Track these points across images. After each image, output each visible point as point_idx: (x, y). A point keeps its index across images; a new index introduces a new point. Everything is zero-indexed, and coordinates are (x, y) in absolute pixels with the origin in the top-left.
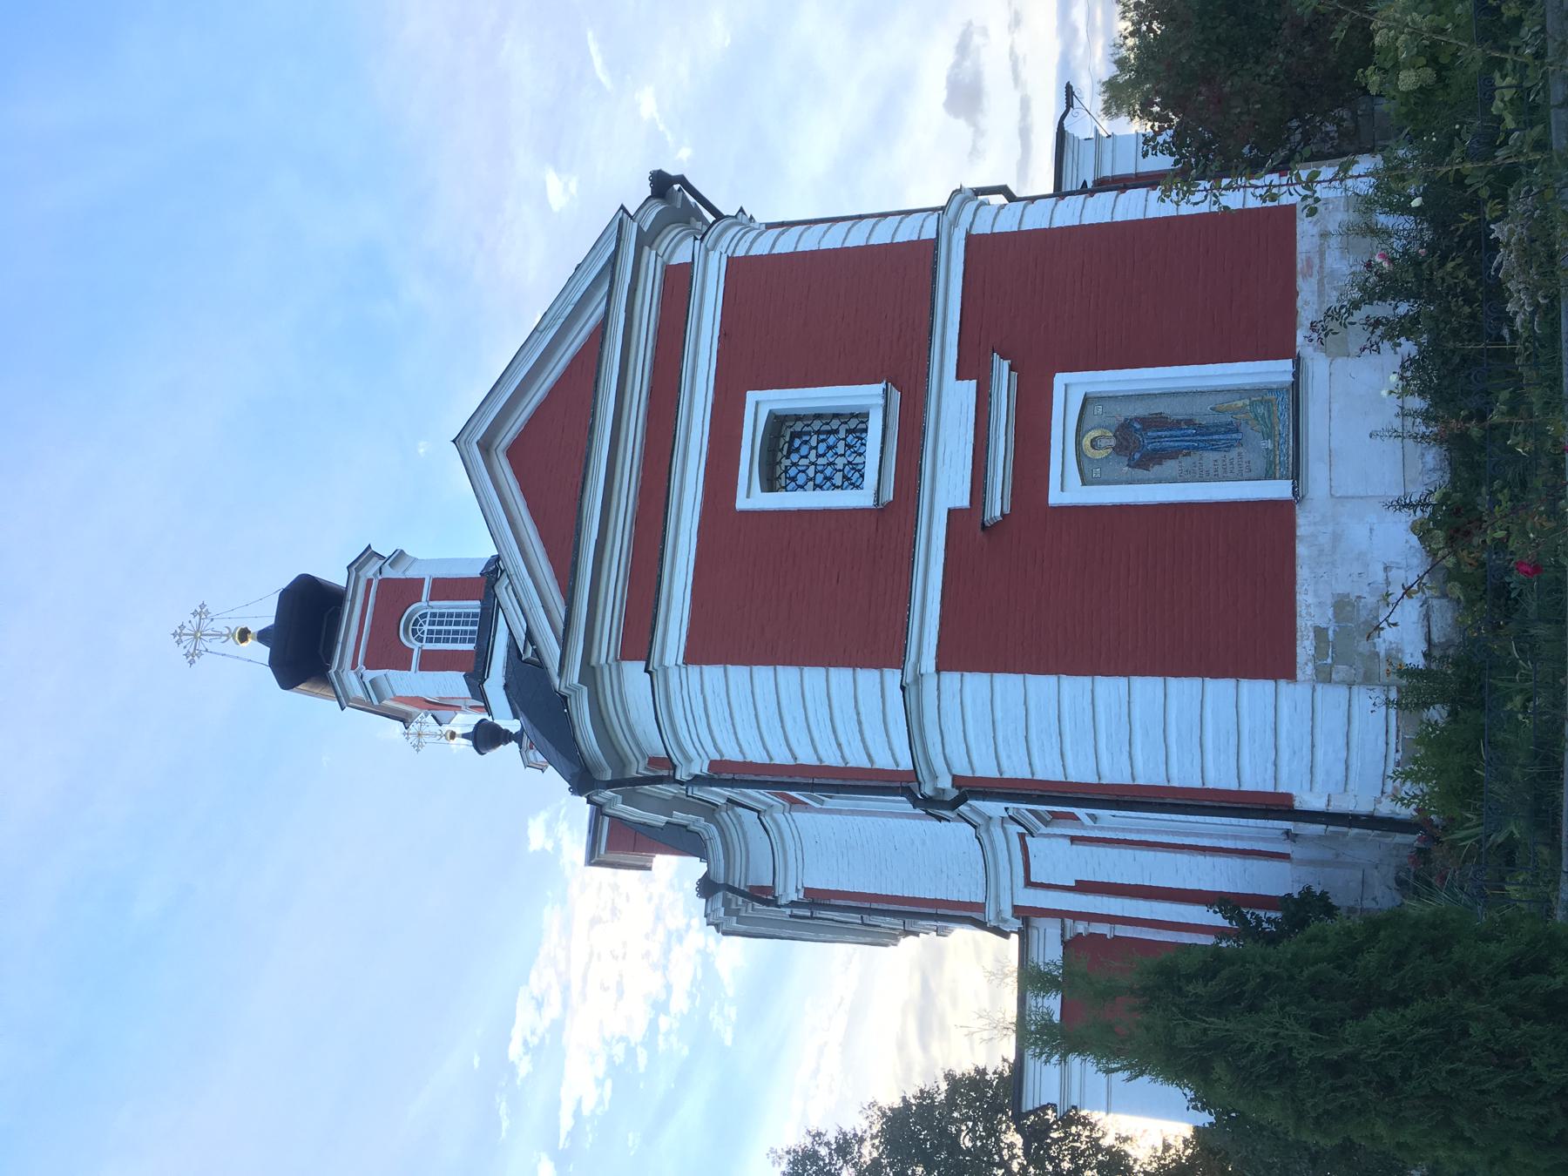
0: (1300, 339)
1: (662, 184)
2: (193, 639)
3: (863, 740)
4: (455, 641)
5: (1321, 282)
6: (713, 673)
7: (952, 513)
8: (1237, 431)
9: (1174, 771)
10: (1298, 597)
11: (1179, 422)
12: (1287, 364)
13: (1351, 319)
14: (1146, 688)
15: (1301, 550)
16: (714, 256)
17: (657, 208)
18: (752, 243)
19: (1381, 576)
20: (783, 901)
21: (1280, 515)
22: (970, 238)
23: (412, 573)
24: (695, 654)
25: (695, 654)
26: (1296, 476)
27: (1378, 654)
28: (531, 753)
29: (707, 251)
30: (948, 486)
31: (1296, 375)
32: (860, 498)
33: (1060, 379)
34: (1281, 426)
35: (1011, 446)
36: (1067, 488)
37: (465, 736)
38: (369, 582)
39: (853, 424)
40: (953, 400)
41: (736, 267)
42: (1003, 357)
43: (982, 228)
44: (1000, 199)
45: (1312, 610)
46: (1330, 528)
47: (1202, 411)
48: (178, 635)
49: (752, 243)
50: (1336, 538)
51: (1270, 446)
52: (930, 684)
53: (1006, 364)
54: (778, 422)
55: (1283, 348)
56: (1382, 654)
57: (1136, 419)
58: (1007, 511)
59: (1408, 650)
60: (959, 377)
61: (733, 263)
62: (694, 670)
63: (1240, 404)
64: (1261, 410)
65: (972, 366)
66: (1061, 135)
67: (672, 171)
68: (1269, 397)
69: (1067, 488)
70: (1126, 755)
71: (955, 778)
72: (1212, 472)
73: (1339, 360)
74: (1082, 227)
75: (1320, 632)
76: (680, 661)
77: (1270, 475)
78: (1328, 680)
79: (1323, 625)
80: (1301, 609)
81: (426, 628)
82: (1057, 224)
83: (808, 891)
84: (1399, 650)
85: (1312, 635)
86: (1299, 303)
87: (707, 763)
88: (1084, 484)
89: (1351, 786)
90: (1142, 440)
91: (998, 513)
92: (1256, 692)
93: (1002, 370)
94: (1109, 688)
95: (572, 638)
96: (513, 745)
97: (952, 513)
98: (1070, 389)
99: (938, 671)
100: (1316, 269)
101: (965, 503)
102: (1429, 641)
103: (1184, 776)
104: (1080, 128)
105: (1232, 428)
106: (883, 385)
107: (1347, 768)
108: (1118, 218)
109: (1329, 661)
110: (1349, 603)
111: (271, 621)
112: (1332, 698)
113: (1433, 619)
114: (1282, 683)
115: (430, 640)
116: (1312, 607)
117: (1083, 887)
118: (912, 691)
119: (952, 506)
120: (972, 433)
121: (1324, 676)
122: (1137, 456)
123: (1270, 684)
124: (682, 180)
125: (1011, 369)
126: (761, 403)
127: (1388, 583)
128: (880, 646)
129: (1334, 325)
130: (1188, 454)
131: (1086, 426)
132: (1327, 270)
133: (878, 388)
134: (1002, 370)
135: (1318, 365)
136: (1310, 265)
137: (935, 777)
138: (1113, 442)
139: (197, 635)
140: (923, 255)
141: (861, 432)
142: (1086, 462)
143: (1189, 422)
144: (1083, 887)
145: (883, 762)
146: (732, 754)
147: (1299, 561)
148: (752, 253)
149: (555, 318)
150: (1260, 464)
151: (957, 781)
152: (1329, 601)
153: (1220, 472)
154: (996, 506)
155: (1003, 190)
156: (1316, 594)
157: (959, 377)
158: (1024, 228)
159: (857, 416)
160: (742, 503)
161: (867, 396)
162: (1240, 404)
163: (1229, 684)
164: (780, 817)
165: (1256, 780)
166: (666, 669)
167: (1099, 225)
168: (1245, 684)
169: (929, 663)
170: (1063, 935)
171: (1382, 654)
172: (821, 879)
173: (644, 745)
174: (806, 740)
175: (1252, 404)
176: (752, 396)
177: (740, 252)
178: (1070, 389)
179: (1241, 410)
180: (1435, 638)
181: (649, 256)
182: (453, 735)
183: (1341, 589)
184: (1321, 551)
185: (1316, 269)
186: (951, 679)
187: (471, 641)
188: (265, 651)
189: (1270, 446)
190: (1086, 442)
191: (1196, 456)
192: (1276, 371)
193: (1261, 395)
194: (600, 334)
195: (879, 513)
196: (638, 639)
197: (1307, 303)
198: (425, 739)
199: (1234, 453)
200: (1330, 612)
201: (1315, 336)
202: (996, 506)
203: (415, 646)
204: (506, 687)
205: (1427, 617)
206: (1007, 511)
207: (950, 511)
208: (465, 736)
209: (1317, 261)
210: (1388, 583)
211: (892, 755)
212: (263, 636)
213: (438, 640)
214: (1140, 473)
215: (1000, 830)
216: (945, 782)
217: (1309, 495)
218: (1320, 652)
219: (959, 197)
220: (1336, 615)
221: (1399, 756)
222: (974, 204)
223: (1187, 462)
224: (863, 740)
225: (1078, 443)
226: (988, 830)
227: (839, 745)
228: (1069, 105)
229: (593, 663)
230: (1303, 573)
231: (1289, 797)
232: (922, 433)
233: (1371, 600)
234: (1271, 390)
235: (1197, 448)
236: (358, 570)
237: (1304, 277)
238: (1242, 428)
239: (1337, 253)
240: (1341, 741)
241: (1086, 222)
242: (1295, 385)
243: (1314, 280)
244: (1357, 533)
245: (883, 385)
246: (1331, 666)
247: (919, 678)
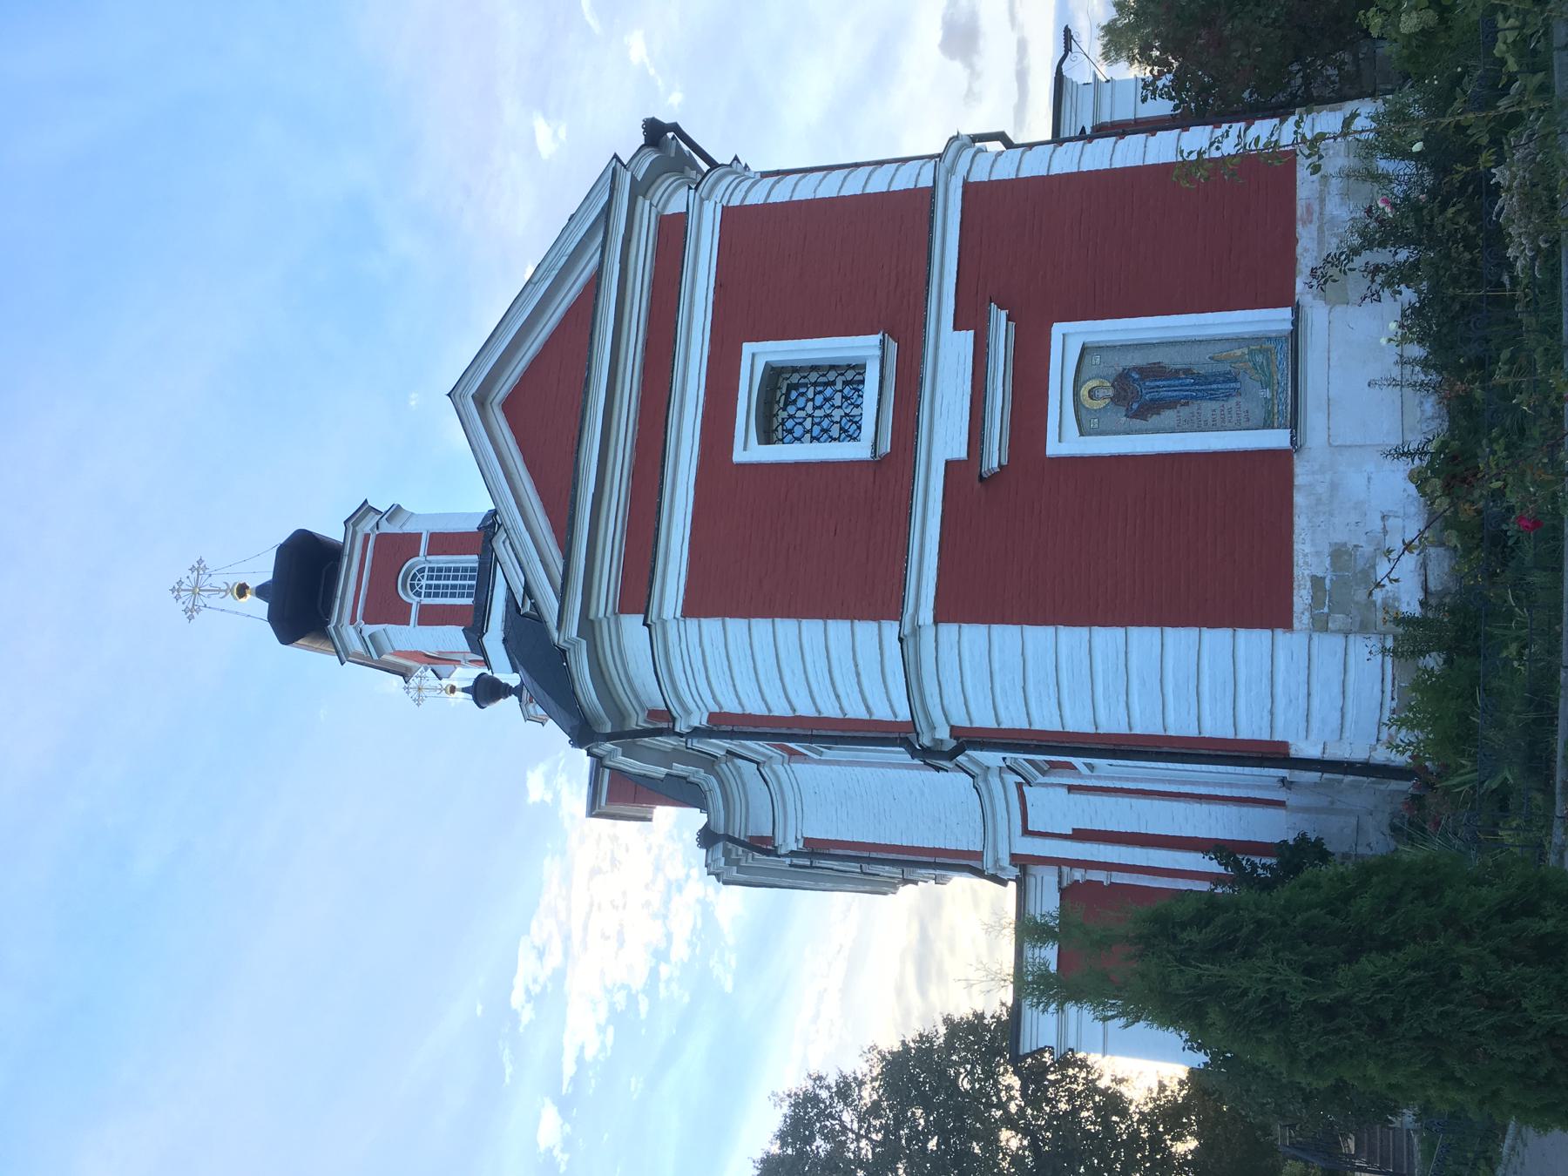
0: (1299, 286)
1: (655, 132)
2: (192, 594)
3: (861, 691)
4: (453, 595)
5: (1320, 229)
6: (711, 626)
7: (950, 465)
8: (1236, 380)
9: (1171, 718)
10: (1296, 547)
11: (1177, 371)
12: (1286, 313)
13: (1350, 265)
14: (1144, 638)
15: (1299, 499)
16: (708, 206)
17: (651, 156)
18: (747, 192)
19: (1378, 524)
20: (782, 851)
21: (1278, 465)
22: (968, 187)
23: (410, 528)
24: (695, 606)
25: (695, 606)
26: (1294, 425)
27: (1374, 603)
28: (530, 707)
29: (702, 200)
30: (945, 437)
31: (1295, 323)
32: (859, 450)
33: (1058, 329)
34: (1280, 373)
35: (1009, 397)
36: (1064, 439)
37: (465, 690)
38: (367, 537)
39: (850, 375)
40: (950, 352)
41: (732, 218)
42: (1001, 307)
43: (980, 175)
44: (995, 146)
45: (1309, 559)
46: (1328, 477)
47: (1200, 360)
48: (176, 590)
49: (747, 192)
50: (1334, 487)
51: (1269, 395)
52: (928, 635)
53: (1003, 314)
54: (774, 374)
55: (1282, 296)
56: (1379, 602)
57: (1134, 368)
58: (1004, 462)
59: (1405, 598)
60: (957, 326)
61: (727, 212)
62: (692, 623)
63: (1238, 352)
64: (1259, 358)
65: (969, 316)
66: (1059, 80)
67: (666, 119)
68: (1267, 345)
69: (1064, 439)
70: (1123, 704)
71: (953, 728)
72: (1210, 423)
73: (1339, 309)
74: (1080, 174)
75: (1317, 582)
76: (678, 614)
77: (1268, 424)
78: (1325, 629)
79: (1320, 574)
80: (1298, 559)
81: (424, 582)
82: (1055, 171)
83: (807, 841)
84: (1396, 599)
85: (1309, 584)
86: (1299, 250)
87: (706, 715)
88: (1082, 434)
89: (1346, 734)
90: (1140, 390)
91: (995, 465)
92: (1253, 642)
93: (999, 320)
94: (1107, 638)
95: (570, 591)
96: (513, 699)
97: (950, 465)
98: (1068, 338)
99: (936, 622)
100: (1315, 216)
101: (961, 453)
102: (1426, 589)
103: (1180, 725)
104: (1079, 73)
105: (1230, 378)
106: (879, 336)
107: (1342, 717)
108: (1117, 164)
109: (1326, 610)
110: (1346, 552)
111: (269, 577)
112: (1328, 646)
113: (1431, 566)
114: (1279, 632)
115: (428, 595)
116: (1309, 556)
117: (1080, 835)
118: (910, 642)
119: (949, 457)
120: (969, 384)
121: (1320, 625)
122: (1135, 406)
123: (1267, 633)
124: (675, 128)
125: (1009, 319)
126: (758, 355)
127: (1385, 532)
128: (877, 597)
129: (1333, 271)
130: (1187, 404)
131: (1083, 377)
132: (1327, 218)
133: (875, 339)
134: (999, 320)
135: (1317, 313)
137: (933, 728)
138: (1111, 393)
139: (196, 591)
140: (920, 203)
141: (857, 384)
142: (1083, 413)
143: (1188, 372)
144: (1080, 835)
145: (882, 713)
146: (731, 706)
147: (1296, 511)
148: (747, 202)
149: (549, 270)
150: (1258, 413)
151: (955, 731)
152: (1327, 550)
153: (1219, 422)
154: (994, 458)
155: (1001, 137)
156: (1313, 543)
157: (957, 326)
158: (1023, 175)
159: (854, 367)
160: (739, 456)
161: (864, 347)
162: (1238, 352)
163: (1225, 633)
164: (779, 768)
165: (1252, 728)
166: (664, 623)
167: (1098, 171)
168: (1242, 633)
169: (926, 615)
170: (1060, 882)
171: (1379, 602)
172: (820, 830)
173: (643, 698)
174: (804, 692)
175: (1251, 352)
176: (748, 348)
177: (735, 202)
178: (1068, 338)
179: (1240, 359)
180: (1432, 586)
181: (643, 205)
182: (453, 689)
183: (1339, 537)
184: (1319, 501)
185: (1315, 216)
186: (949, 630)
187: (469, 595)
188: (263, 607)
189: (1269, 395)
190: (1084, 392)
191: (1194, 407)
192: (1275, 319)
193: (1259, 344)
194: (594, 285)
195: (877, 464)
196: (636, 593)
197: (1306, 250)
198: (425, 693)
199: (1232, 402)
200: (1327, 562)
201: (1315, 283)
202: (994, 458)
203: (414, 601)
204: (505, 641)
205: (1424, 566)
206: (1004, 462)
207: (948, 463)
208: (465, 690)
209: (1316, 208)
210: (1385, 532)
211: (890, 706)
212: (261, 592)
213: (436, 595)
214: (1138, 423)
215: (998, 780)
216: (943, 733)
217: (1308, 444)
218: (1316, 601)
219: (956, 144)
220: (1333, 564)
221: (1394, 704)
222: (972, 151)
223: (1185, 412)
224: (861, 691)
225: (1076, 394)
226: (986, 781)
227: (838, 697)
228: (1068, 49)
229: (592, 616)
230: (1300, 522)
231: (1285, 745)
232: (920, 384)
233: (1368, 549)
234: (1269, 339)
235: (1196, 398)
236: (354, 525)
237: (1304, 224)
238: (1240, 377)
239: (1337, 199)
240: (1337, 689)
241: (1084, 169)
242: (1294, 333)
243: (1314, 227)
244: (1354, 482)
245: (879, 336)
246: (1328, 615)
247: (916, 629)
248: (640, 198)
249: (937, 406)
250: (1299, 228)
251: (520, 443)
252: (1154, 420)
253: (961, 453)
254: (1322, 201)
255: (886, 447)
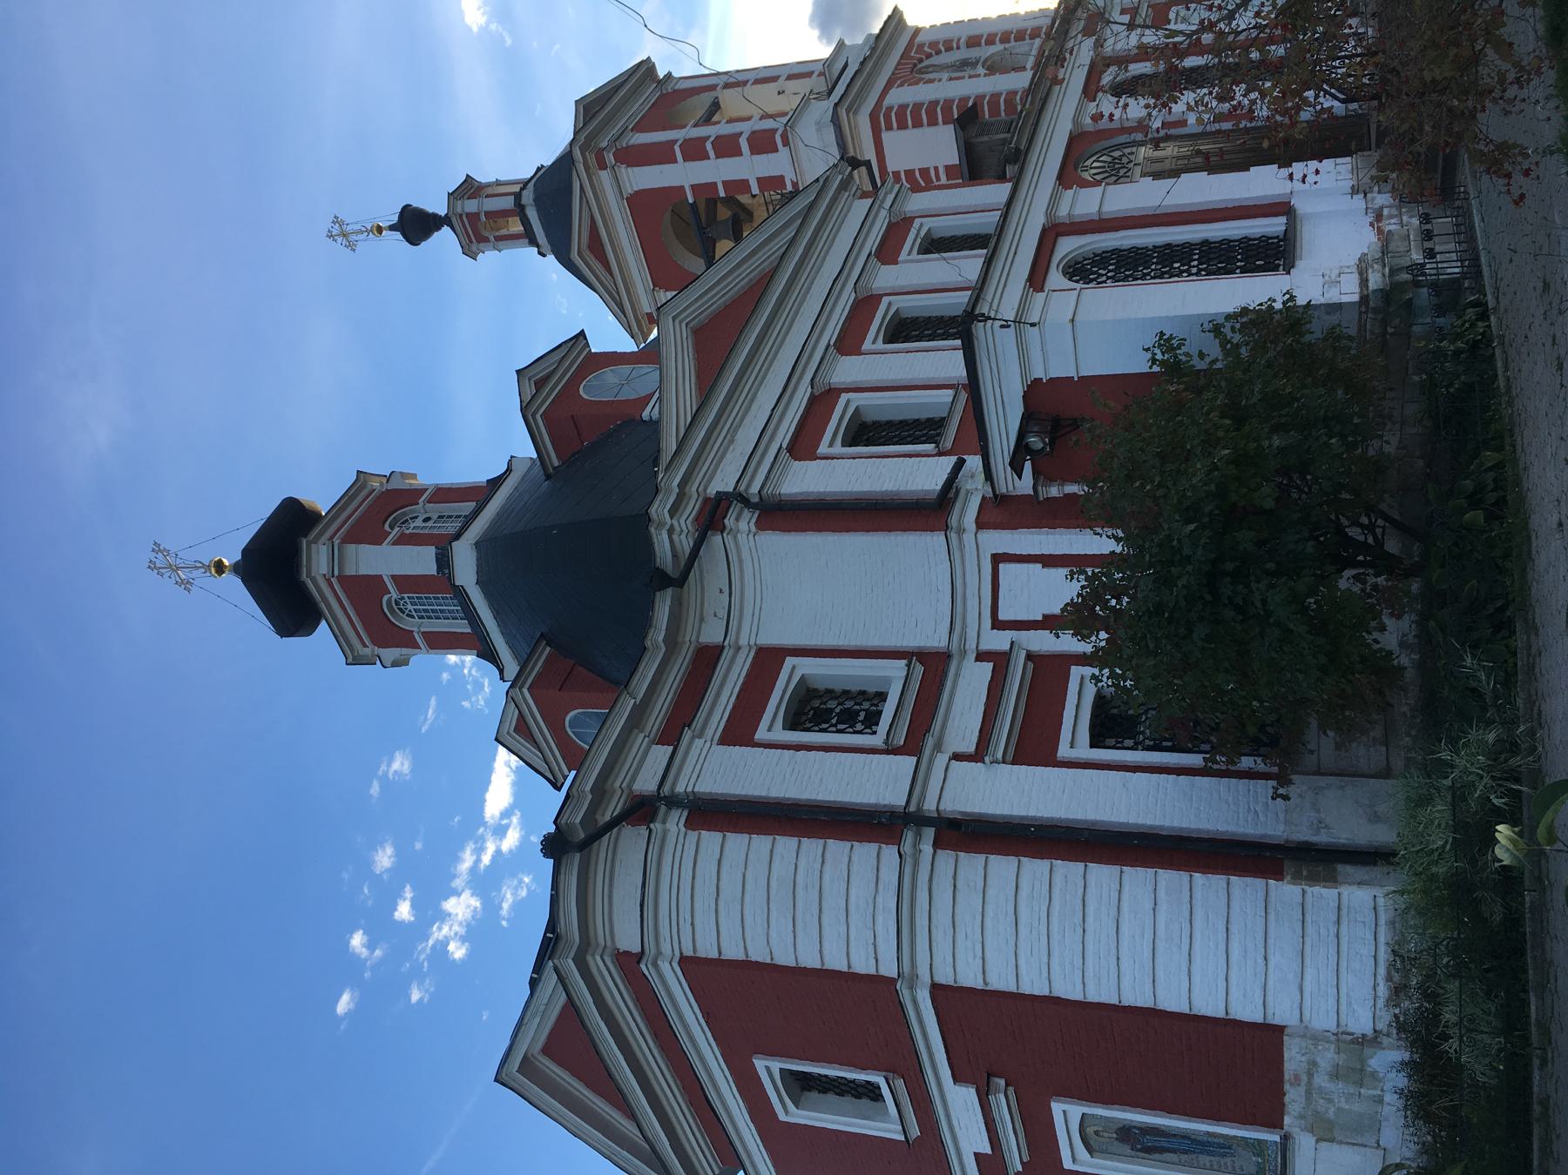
0: (1287, 1120)
5: (1308, 1093)
16: (665, 966)
37: (392, 228)
73: (1323, 1144)
81: (410, 607)
86: (1287, 1099)
96: (446, 229)
111: (239, 557)
136: (1297, 1078)
143: (1184, 1137)
157: (957, 1079)
181: (596, 963)
182: (380, 230)
199: (1228, 1160)
208: (392, 228)
209: (1304, 1078)
212: (236, 568)
223: (1184, 1157)
243: (1302, 1089)
248: (589, 958)
249: (955, 1123)
250: (1287, 1087)
251: (574, 1074)
252: (1157, 1156)
253: (986, 1149)
254: (1310, 1075)
255: (915, 1132)
